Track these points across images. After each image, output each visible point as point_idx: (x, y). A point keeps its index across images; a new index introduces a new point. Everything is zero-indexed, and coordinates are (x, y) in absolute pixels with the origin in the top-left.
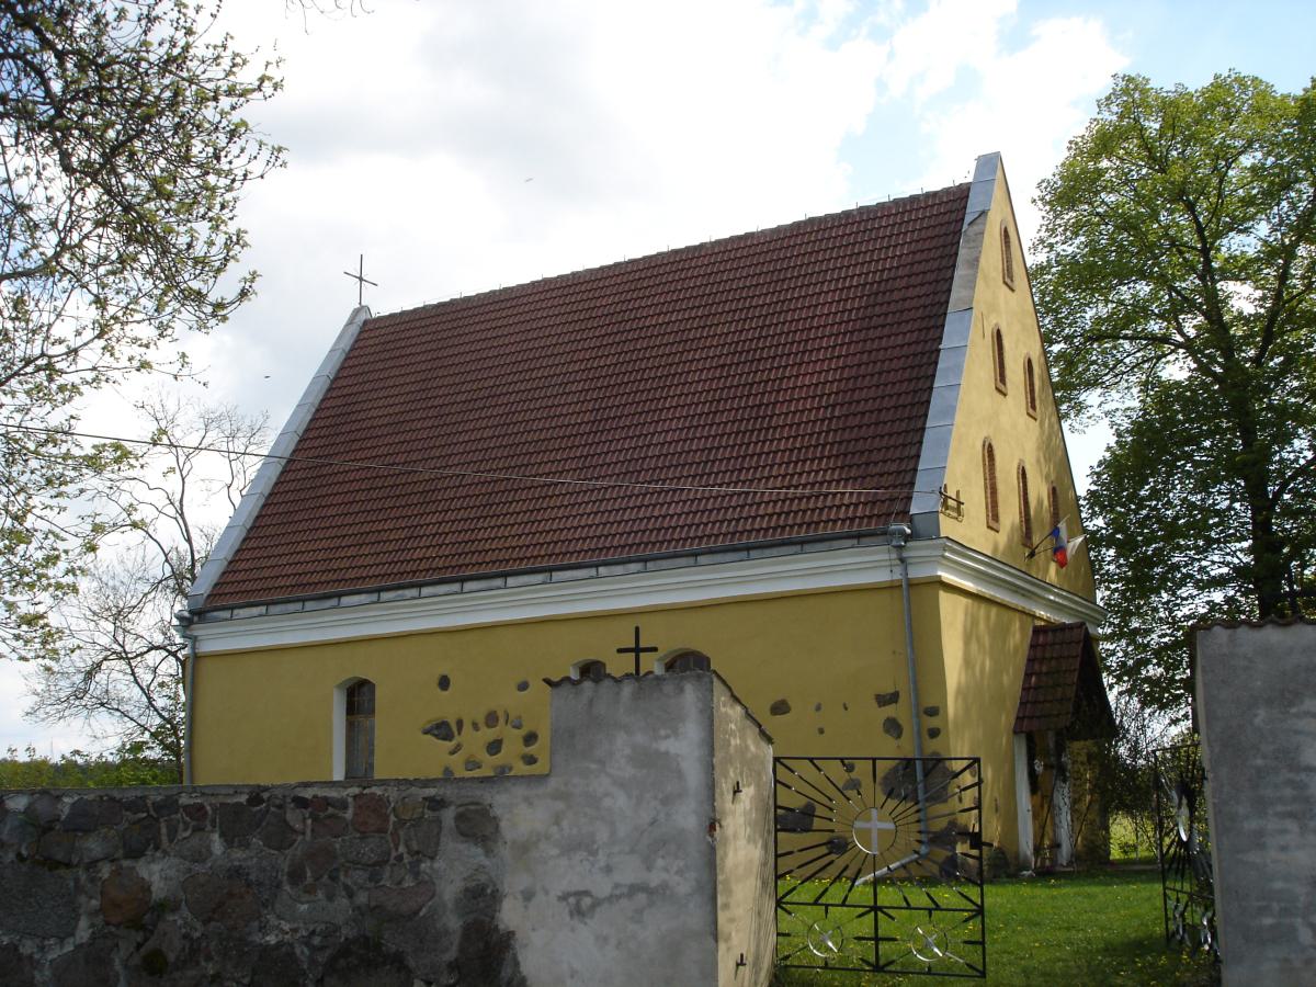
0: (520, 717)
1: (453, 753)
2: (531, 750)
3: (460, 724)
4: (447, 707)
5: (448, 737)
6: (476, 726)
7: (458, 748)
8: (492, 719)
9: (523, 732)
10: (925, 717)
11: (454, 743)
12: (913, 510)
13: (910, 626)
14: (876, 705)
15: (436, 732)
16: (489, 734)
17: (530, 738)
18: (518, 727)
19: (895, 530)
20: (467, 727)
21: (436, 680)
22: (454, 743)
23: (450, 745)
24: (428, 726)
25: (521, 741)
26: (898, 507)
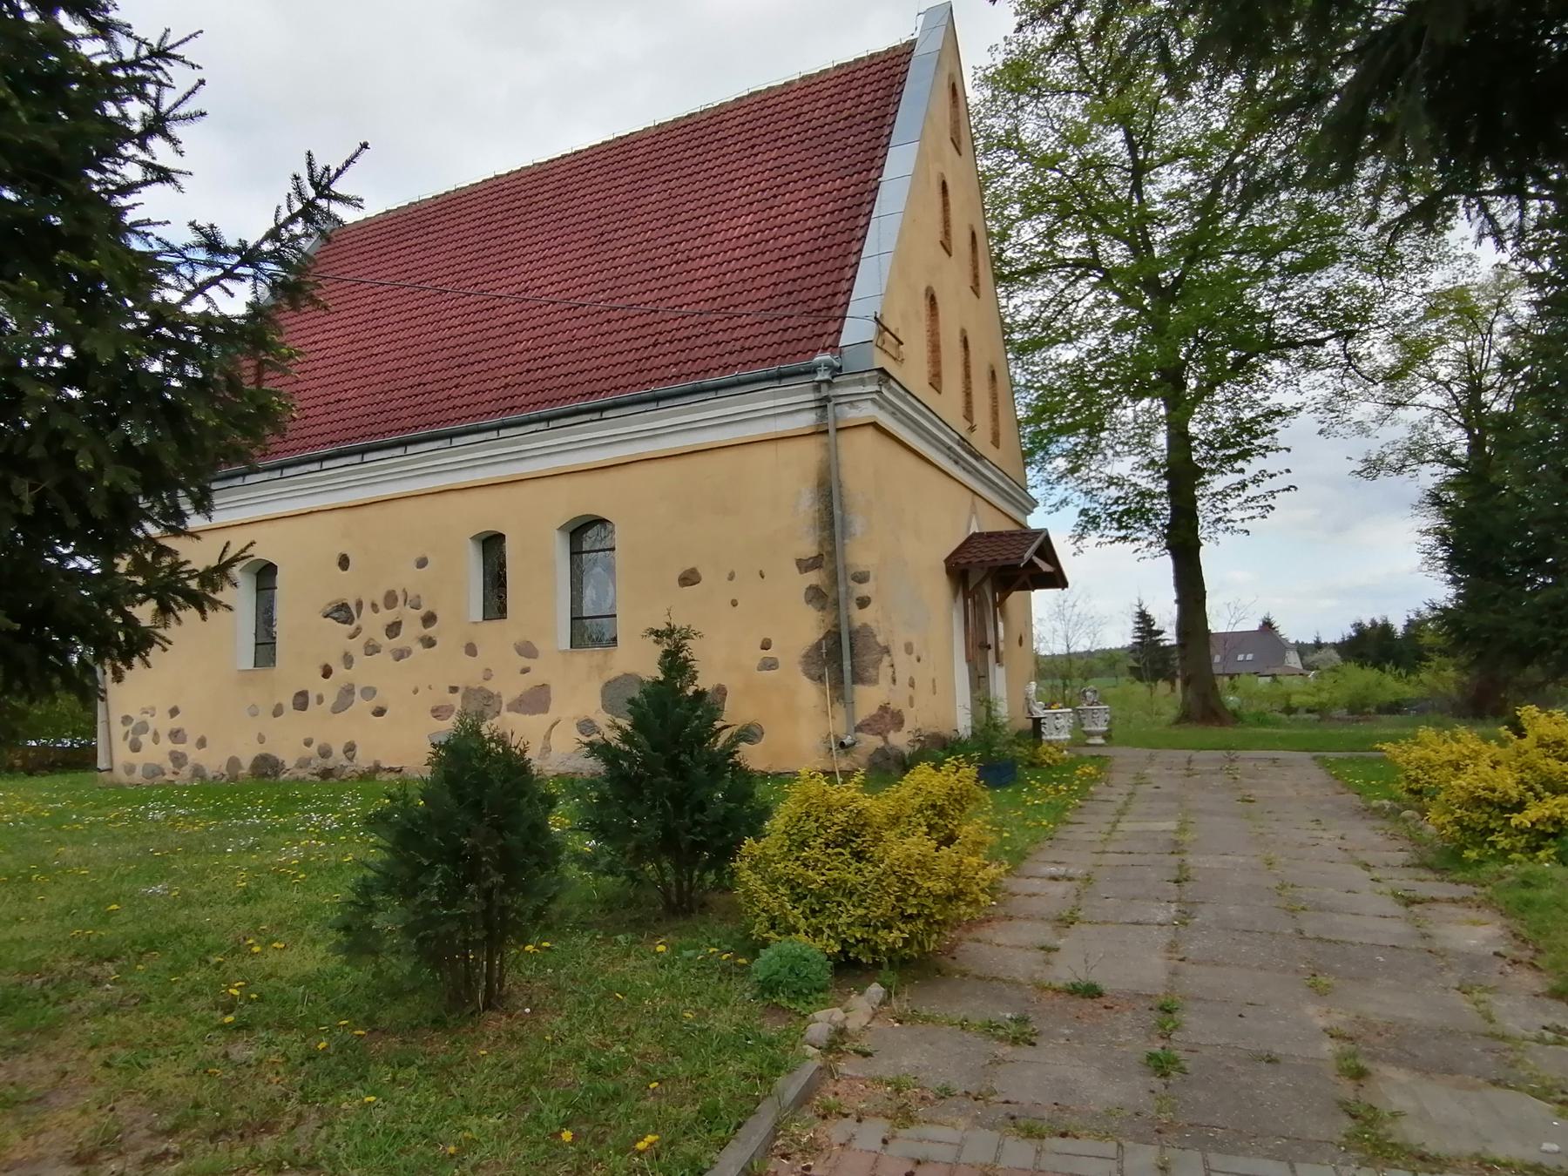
0: (418, 597)
1: (352, 637)
2: (431, 631)
3: (359, 605)
4: (347, 588)
5: (348, 620)
6: (374, 607)
7: (359, 630)
8: (391, 600)
9: (422, 612)
10: (852, 584)
11: (354, 626)
12: (844, 340)
13: (189, 94)
14: (796, 570)
15: (336, 615)
16: (388, 616)
17: (429, 619)
18: (417, 607)
19: (821, 361)
20: (366, 609)
21: (336, 561)
22: (354, 626)
23: (350, 628)
24: (329, 609)
25: (420, 622)
26: (830, 341)
